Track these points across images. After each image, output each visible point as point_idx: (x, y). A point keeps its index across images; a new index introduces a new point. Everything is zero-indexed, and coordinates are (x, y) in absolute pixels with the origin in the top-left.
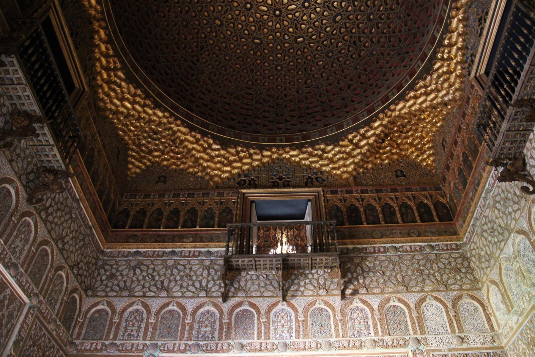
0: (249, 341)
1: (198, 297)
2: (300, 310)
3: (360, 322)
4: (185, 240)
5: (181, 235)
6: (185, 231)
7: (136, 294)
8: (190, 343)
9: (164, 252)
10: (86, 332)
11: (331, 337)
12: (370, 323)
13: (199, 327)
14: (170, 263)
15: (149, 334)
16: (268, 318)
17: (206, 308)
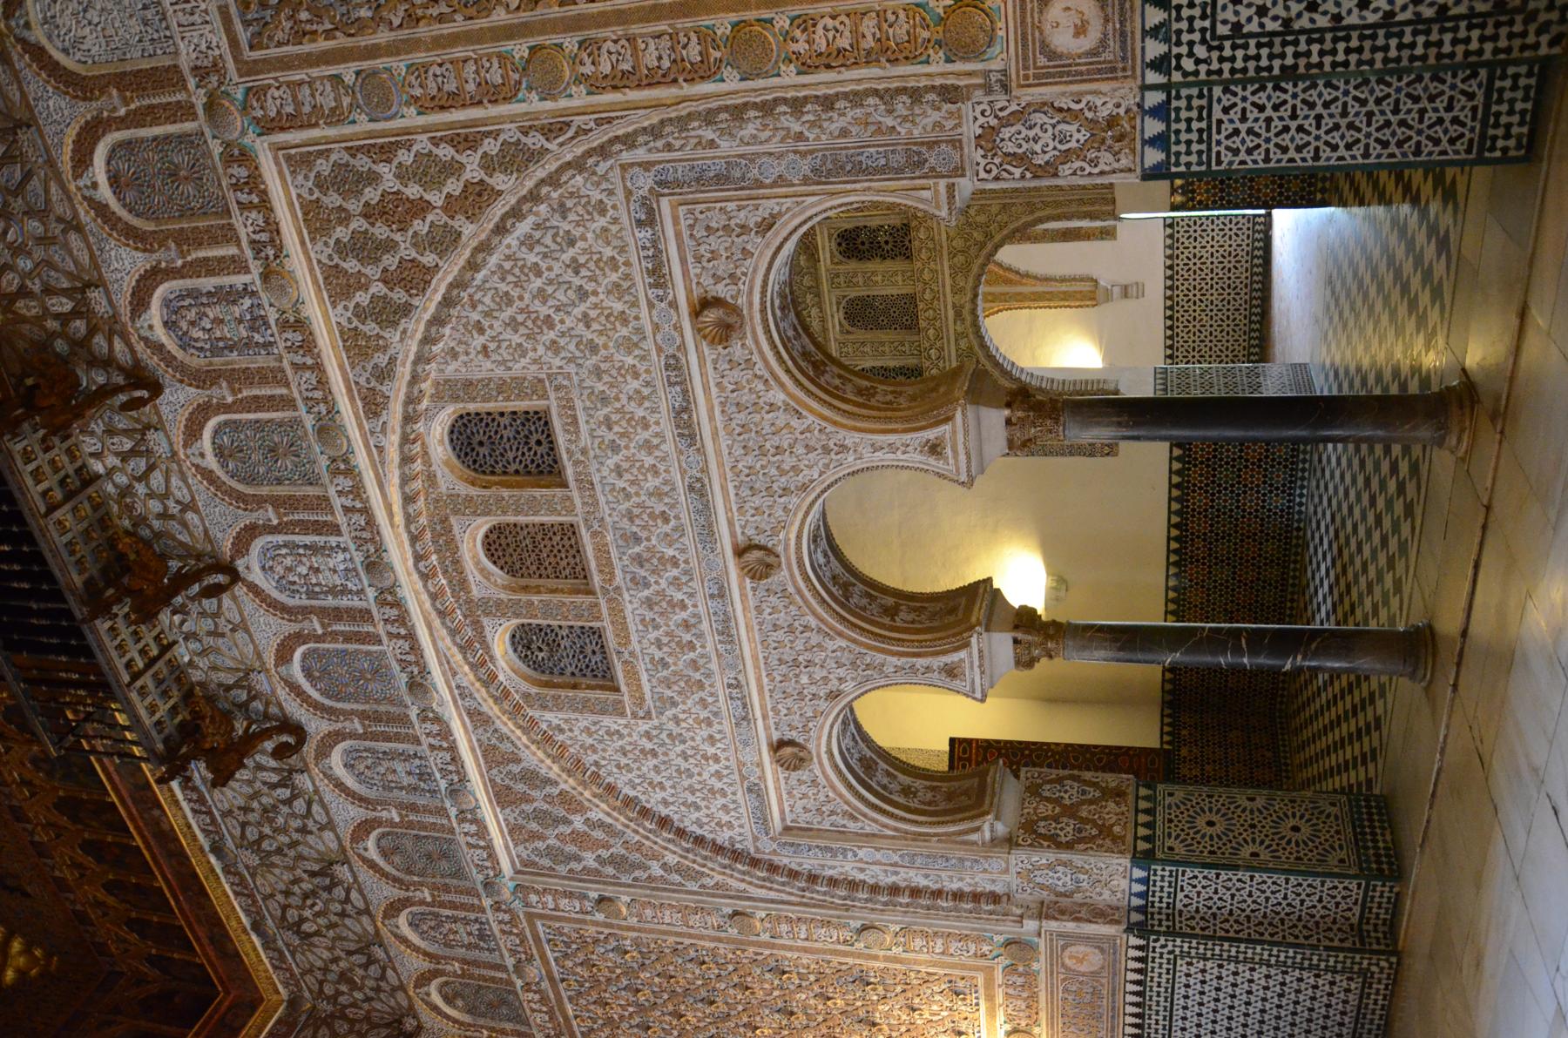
0: (396, 667)
1: (316, 791)
2: (247, 519)
3: (218, 321)
4: (165, 827)
5: (155, 836)
6: (137, 827)
7: (370, 929)
8: (453, 812)
9: (226, 871)
10: (509, 1020)
11: (298, 422)
12: (208, 283)
13: (402, 788)
14: (254, 860)
15: (464, 899)
16: (306, 612)
17: (340, 771)
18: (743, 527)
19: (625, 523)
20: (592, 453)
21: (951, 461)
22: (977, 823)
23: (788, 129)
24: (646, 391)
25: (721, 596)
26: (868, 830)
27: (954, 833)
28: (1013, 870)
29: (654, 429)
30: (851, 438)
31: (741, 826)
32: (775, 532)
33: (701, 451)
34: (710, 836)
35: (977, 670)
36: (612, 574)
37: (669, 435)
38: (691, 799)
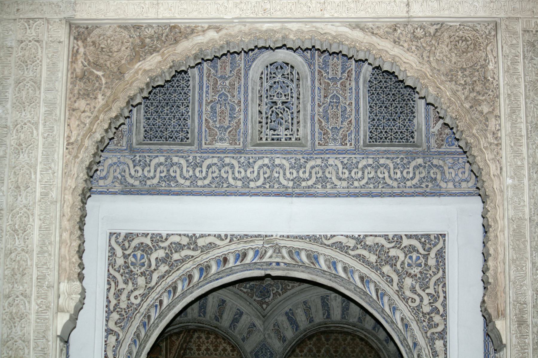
31: (199, 354)
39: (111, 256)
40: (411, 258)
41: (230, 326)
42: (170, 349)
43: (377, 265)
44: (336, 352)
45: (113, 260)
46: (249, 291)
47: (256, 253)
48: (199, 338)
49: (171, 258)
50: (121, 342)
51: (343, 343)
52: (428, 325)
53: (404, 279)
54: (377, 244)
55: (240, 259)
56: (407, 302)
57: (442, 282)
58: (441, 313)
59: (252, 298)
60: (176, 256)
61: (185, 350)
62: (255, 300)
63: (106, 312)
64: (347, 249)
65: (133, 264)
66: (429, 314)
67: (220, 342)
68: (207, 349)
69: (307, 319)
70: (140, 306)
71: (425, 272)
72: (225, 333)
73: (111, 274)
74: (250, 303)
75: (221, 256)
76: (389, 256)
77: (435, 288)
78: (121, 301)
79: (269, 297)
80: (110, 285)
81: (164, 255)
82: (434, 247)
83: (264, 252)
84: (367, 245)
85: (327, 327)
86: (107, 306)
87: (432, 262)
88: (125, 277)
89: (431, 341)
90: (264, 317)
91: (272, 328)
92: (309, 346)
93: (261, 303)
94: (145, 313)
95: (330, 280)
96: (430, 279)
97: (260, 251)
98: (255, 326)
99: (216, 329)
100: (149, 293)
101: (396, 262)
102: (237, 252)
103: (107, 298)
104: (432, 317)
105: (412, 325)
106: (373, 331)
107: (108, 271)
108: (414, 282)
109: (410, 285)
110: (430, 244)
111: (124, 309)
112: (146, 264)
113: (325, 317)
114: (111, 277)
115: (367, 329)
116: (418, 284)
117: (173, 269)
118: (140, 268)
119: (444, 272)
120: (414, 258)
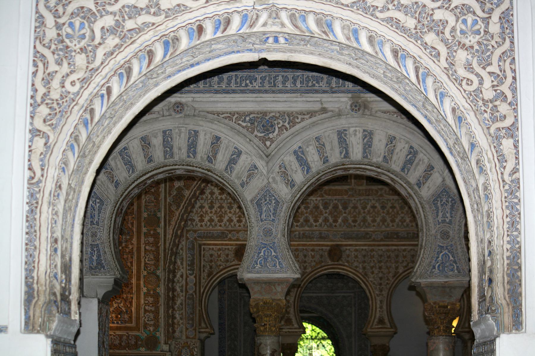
18: (349, 249)
19: (351, 205)
20: (381, 198)
21: (377, 327)
22: (208, 326)
23: (368, 204)
24: (405, 224)
25: (322, 237)
26: (203, 281)
27: (203, 317)
28: (189, 340)
29: (391, 224)
30: (385, 293)
31: (201, 226)
32: (348, 262)
33: (382, 240)
34: (194, 210)
35: (287, 330)
36: (329, 195)
37: (388, 229)
38: (216, 206)
39: (39, 27)
40: (465, 22)
41: (226, 169)
42: (169, 221)
43: (417, 33)
44: (355, 221)
45: (42, 33)
46: (249, 125)
47: (244, 18)
48: (202, 207)
49: (123, 26)
50: (52, 146)
51: (362, 211)
52: (490, 118)
53: (456, 52)
54: (416, 3)
55: (222, 28)
56: (461, 85)
57: (509, 56)
58: (509, 101)
59: (252, 133)
60: (130, 24)
61: (186, 221)
62: (256, 136)
63: (31, 105)
64: (374, 10)
65: (68, 36)
66: (491, 101)
67: (226, 212)
68: (211, 220)
69: (321, 159)
70: (78, 95)
71: (485, 42)
72: (220, 177)
73: (38, 52)
74: (250, 140)
75: (194, 23)
76: (434, 20)
77: (499, 66)
78: (51, 90)
79: (273, 132)
80: (37, 67)
81: (113, 23)
82: (497, 7)
83: (255, 17)
84: (403, 5)
85: (345, 169)
86: (32, 97)
87: (495, 28)
88: (58, 55)
89: (497, 139)
90: (267, 157)
91: (277, 170)
92: (325, 215)
93: (263, 140)
94: (85, 105)
95: (350, 64)
96: (492, 53)
97: (250, 16)
98: (257, 169)
99: (210, 173)
100: (91, 77)
101: (444, 28)
102: (217, 18)
103: (33, 85)
104: (496, 106)
105: (468, 117)
106: (402, 173)
107: (35, 47)
108: (469, 57)
109: (464, 60)
110: (492, 4)
111: (57, 100)
112: (87, 35)
113: (342, 156)
114: (38, 55)
115: (394, 171)
116: (476, 58)
117: (125, 42)
118: (79, 42)
119: (512, 42)
120: (469, 22)
